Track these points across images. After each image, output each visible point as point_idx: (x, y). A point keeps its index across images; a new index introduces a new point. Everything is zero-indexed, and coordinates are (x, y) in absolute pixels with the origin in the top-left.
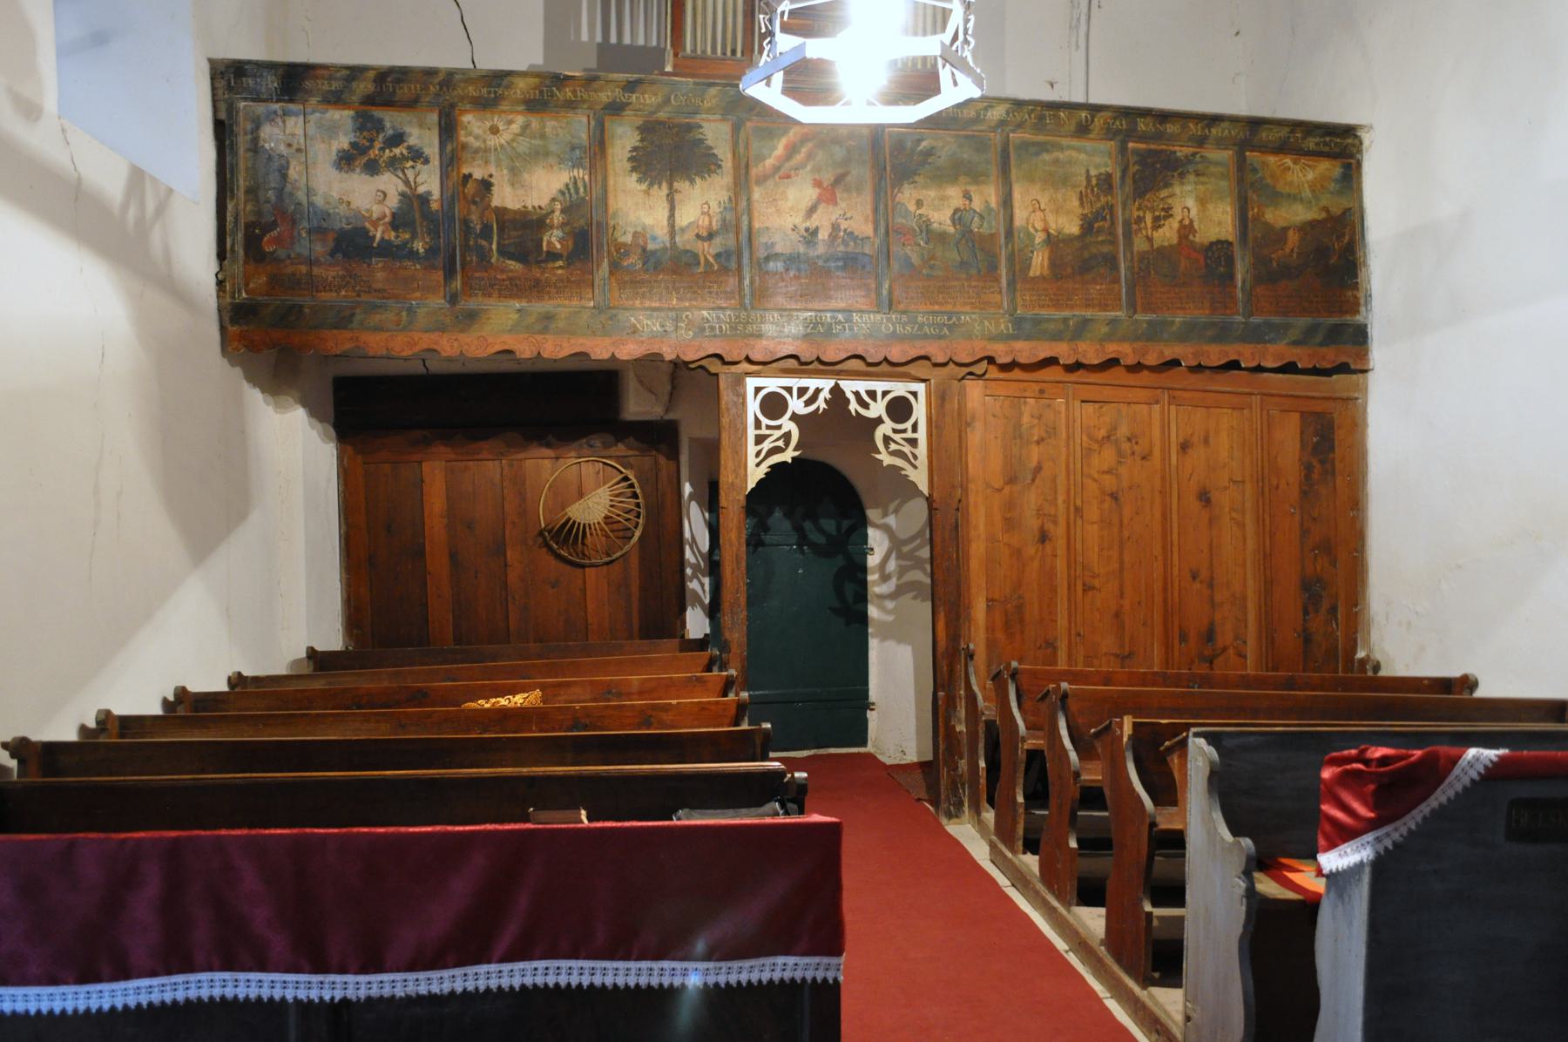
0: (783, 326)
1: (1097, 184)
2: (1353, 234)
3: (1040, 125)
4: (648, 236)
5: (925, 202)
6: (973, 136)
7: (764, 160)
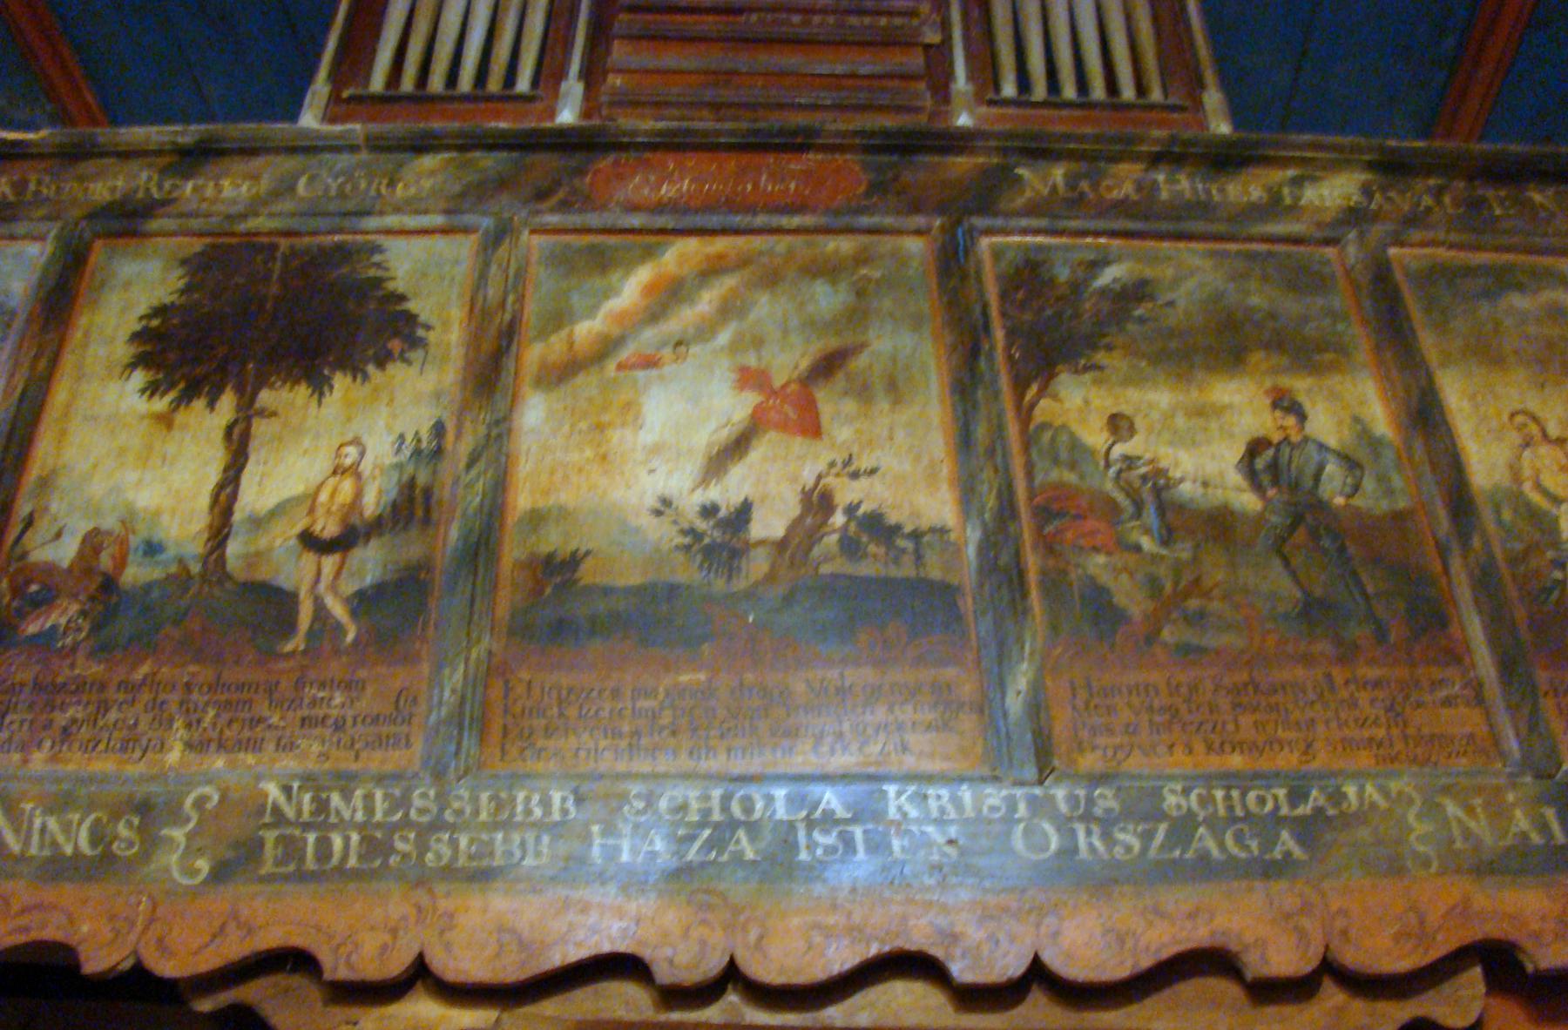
0: (587, 838)
4: (134, 541)
5: (1139, 423)
6: (1270, 254)
7: (573, 322)
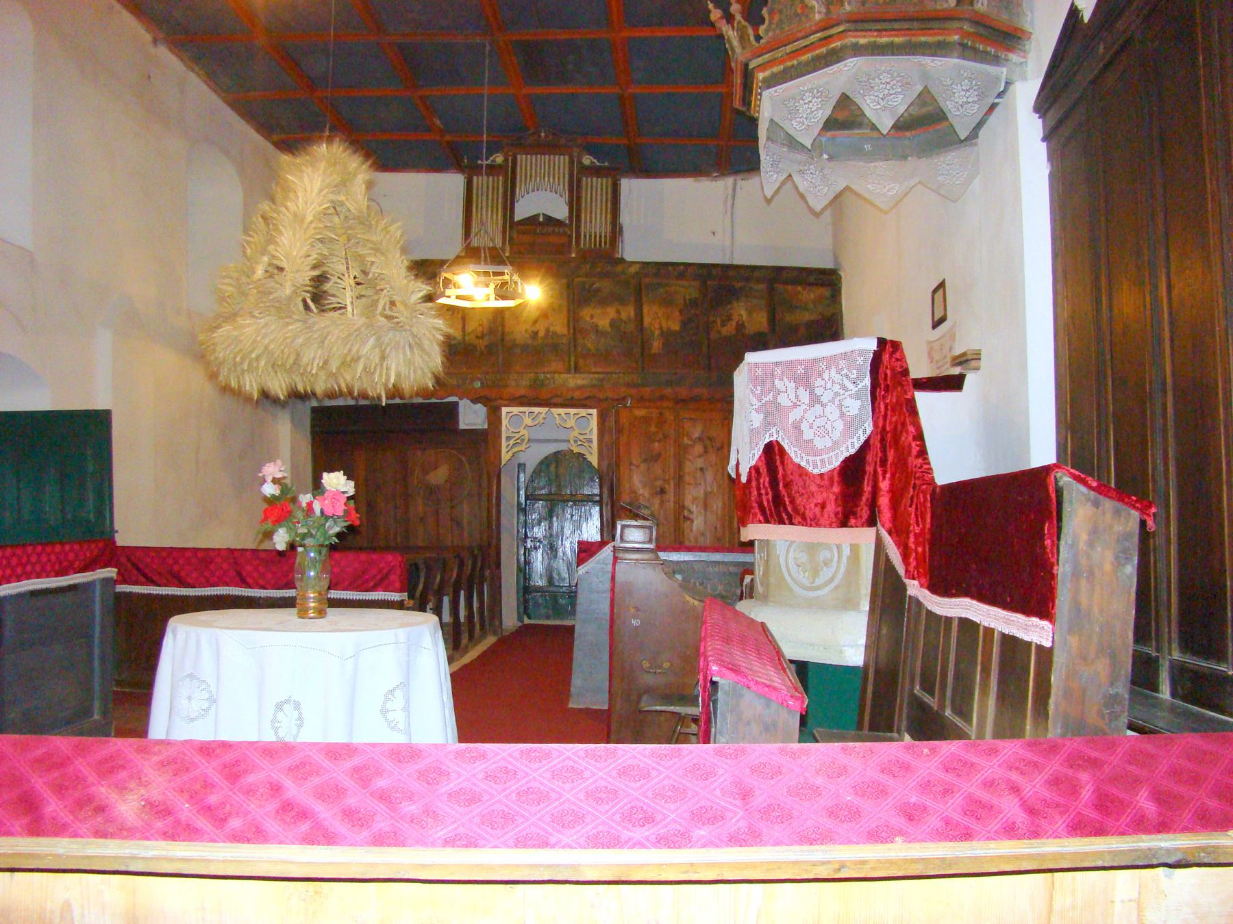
1: (690, 303)
2: (837, 329)
3: (657, 275)
